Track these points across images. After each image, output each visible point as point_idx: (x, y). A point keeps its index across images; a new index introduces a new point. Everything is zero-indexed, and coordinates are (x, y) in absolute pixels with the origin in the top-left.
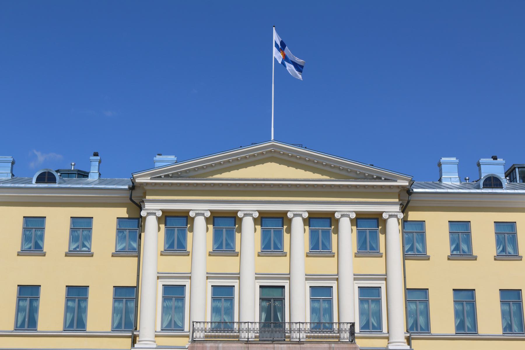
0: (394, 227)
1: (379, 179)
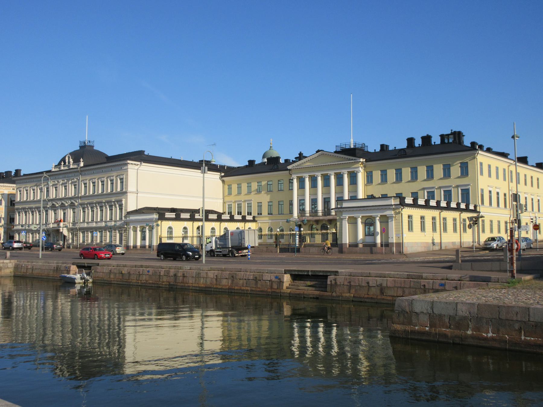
1: (352, 160)
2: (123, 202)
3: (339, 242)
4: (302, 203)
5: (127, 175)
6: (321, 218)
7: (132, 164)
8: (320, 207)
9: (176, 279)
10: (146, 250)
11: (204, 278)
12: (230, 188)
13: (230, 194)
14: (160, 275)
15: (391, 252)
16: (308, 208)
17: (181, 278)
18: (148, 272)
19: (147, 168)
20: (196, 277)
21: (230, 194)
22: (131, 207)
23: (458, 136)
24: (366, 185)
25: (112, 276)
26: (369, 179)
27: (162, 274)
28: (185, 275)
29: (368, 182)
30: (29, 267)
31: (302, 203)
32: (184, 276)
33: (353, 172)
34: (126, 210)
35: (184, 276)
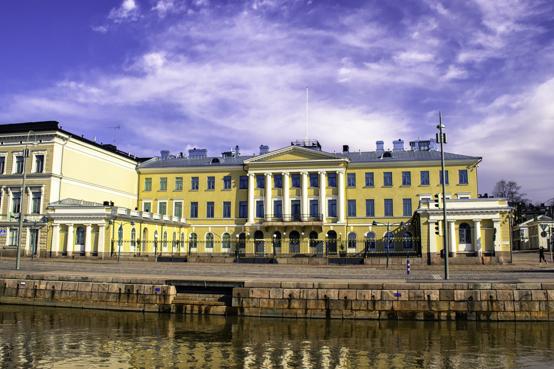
2: (43, 189)
4: (261, 206)
5: (52, 151)
6: (270, 224)
7: (59, 137)
8: (287, 210)
9: (472, 305)
10: (86, 258)
11: (540, 301)
12: (149, 181)
13: (149, 188)
14: (429, 301)
15: (498, 262)
16: (270, 210)
17: (484, 304)
18: (398, 295)
19: (73, 145)
20: (520, 300)
21: (149, 188)
22: (54, 198)
24: (346, 188)
25: (295, 304)
26: (351, 182)
27: (435, 296)
28: (495, 298)
29: (349, 185)
30: (43, 287)
31: (261, 206)
32: (491, 300)
33: (334, 173)
34: (47, 200)
35: (491, 300)
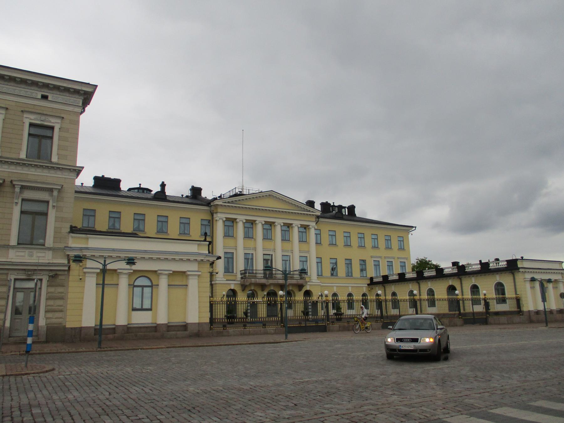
0: (312, 232)
1: (309, 211)
3: (525, 309)
23: (352, 209)
